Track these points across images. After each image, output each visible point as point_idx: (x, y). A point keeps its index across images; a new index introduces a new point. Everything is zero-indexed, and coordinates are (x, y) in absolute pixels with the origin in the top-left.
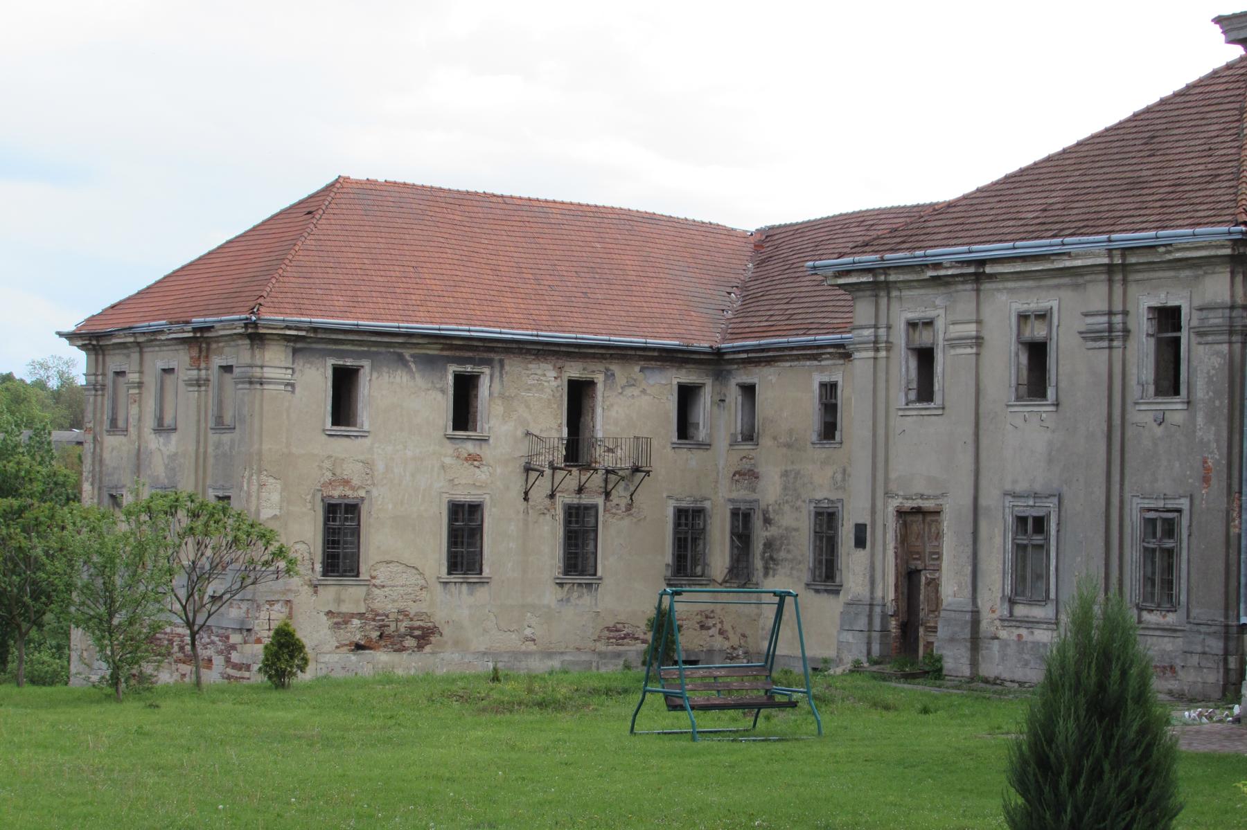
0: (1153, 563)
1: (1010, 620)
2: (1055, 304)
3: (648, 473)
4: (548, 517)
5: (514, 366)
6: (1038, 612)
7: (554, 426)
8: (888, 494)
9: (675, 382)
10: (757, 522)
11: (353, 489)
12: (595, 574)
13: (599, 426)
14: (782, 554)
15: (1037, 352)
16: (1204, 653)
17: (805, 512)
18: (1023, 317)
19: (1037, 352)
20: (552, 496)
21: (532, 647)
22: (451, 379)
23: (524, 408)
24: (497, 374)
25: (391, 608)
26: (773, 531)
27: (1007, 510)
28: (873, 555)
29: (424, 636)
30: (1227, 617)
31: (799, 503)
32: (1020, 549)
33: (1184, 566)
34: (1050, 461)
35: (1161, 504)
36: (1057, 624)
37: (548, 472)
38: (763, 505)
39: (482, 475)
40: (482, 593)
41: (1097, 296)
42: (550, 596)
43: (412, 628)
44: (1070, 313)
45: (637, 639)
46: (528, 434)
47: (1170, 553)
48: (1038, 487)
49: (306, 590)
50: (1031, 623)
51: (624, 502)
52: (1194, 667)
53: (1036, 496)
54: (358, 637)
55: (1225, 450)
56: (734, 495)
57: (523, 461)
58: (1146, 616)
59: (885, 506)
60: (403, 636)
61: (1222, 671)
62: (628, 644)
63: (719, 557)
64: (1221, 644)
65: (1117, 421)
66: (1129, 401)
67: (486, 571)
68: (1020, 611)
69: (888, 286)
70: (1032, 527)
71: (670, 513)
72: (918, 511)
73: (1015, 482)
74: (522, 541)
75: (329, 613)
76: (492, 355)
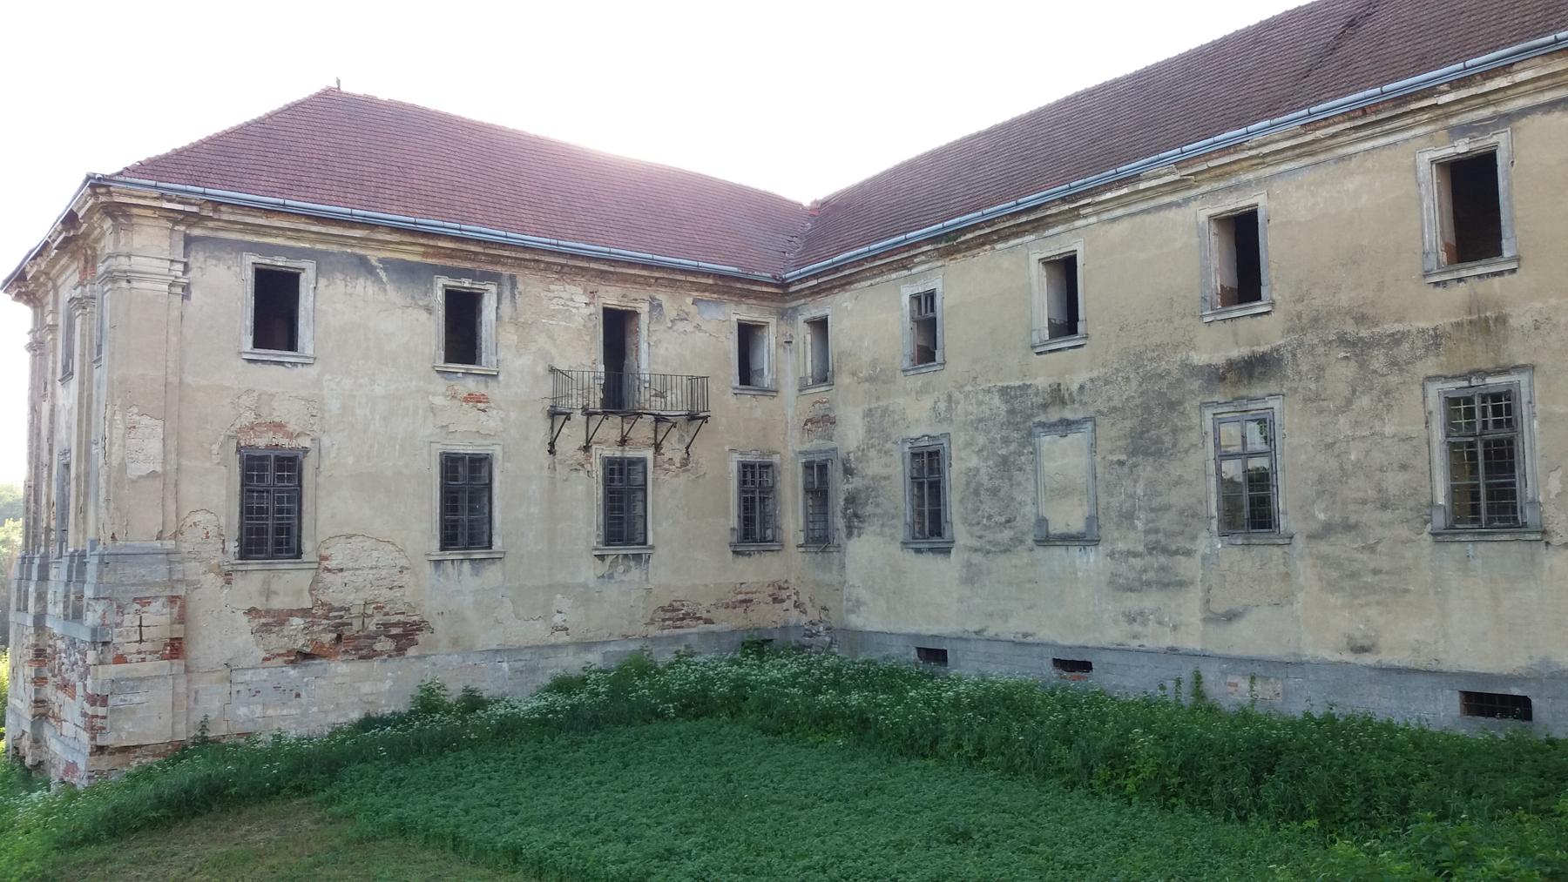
3: (705, 419)
4: (582, 474)
5: (530, 285)
7: (585, 357)
9: (734, 318)
10: (835, 473)
11: (290, 436)
12: (645, 543)
13: (644, 365)
14: (869, 509)
17: (897, 456)
20: (586, 448)
21: (562, 638)
22: (439, 297)
23: (544, 332)
24: (507, 293)
25: (354, 599)
26: (856, 483)
29: (406, 635)
31: (889, 445)
37: (578, 417)
38: (842, 453)
39: (491, 422)
42: (588, 571)
43: (387, 626)
45: (700, 618)
46: (552, 370)
49: (211, 581)
51: (678, 457)
54: (300, 643)
56: (807, 447)
57: (548, 404)
60: (373, 637)
62: (689, 626)
63: (791, 515)
67: (497, 543)
71: (733, 468)
74: (546, 502)
75: (252, 612)
76: (499, 269)
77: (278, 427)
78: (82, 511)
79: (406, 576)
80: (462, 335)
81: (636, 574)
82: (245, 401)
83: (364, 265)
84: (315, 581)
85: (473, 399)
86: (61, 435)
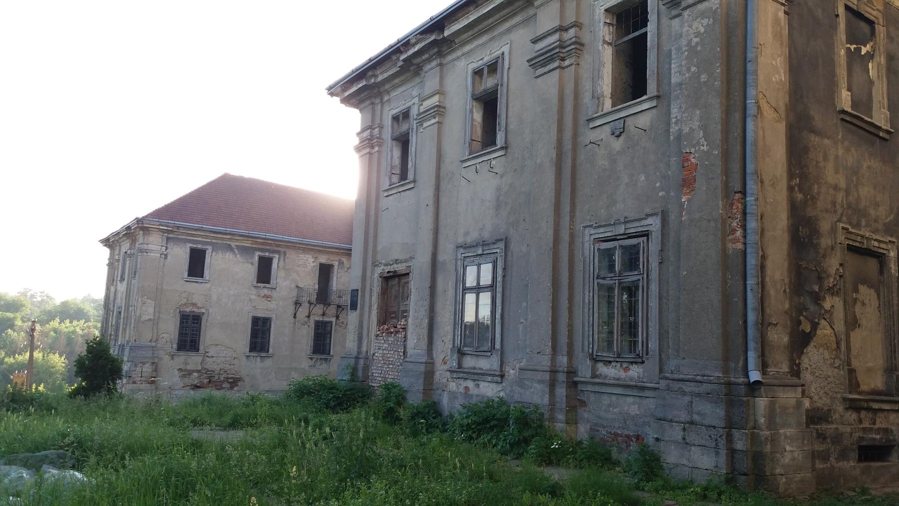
0: (610, 303)
1: (459, 372)
2: (506, 49)
5: (291, 255)
6: (484, 364)
7: (311, 283)
8: (375, 265)
11: (198, 308)
13: (334, 285)
15: (489, 104)
16: (692, 423)
19: (489, 104)
20: (309, 317)
22: (257, 258)
24: (282, 258)
25: (217, 368)
27: (459, 263)
28: (361, 316)
29: (234, 382)
30: (726, 371)
33: (654, 303)
34: (498, 207)
35: (621, 230)
36: (502, 376)
37: (307, 305)
39: (272, 305)
40: (268, 362)
46: (298, 287)
47: (631, 290)
48: (486, 235)
49: (167, 358)
50: (477, 375)
52: (676, 442)
53: (484, 244)
55: (718, 137)
57: (295, 299)
58: (602, 369)
59: (373, 273)
60: (223, 382)
61: (723, 452)
64: (721, 412)
65: (568, 146)
66: (582, 119)
67: (271, 350)
73: (467, 234)
74: (291, 338)
77: (194, 305)
78: (124, 330)
79: (236, 361)
80: (264, 274)
81: (324, 366)
82: (184, 295)
83: (229, 248)
84: (203, 360)
85: (266, 297)
86: (118, 301)
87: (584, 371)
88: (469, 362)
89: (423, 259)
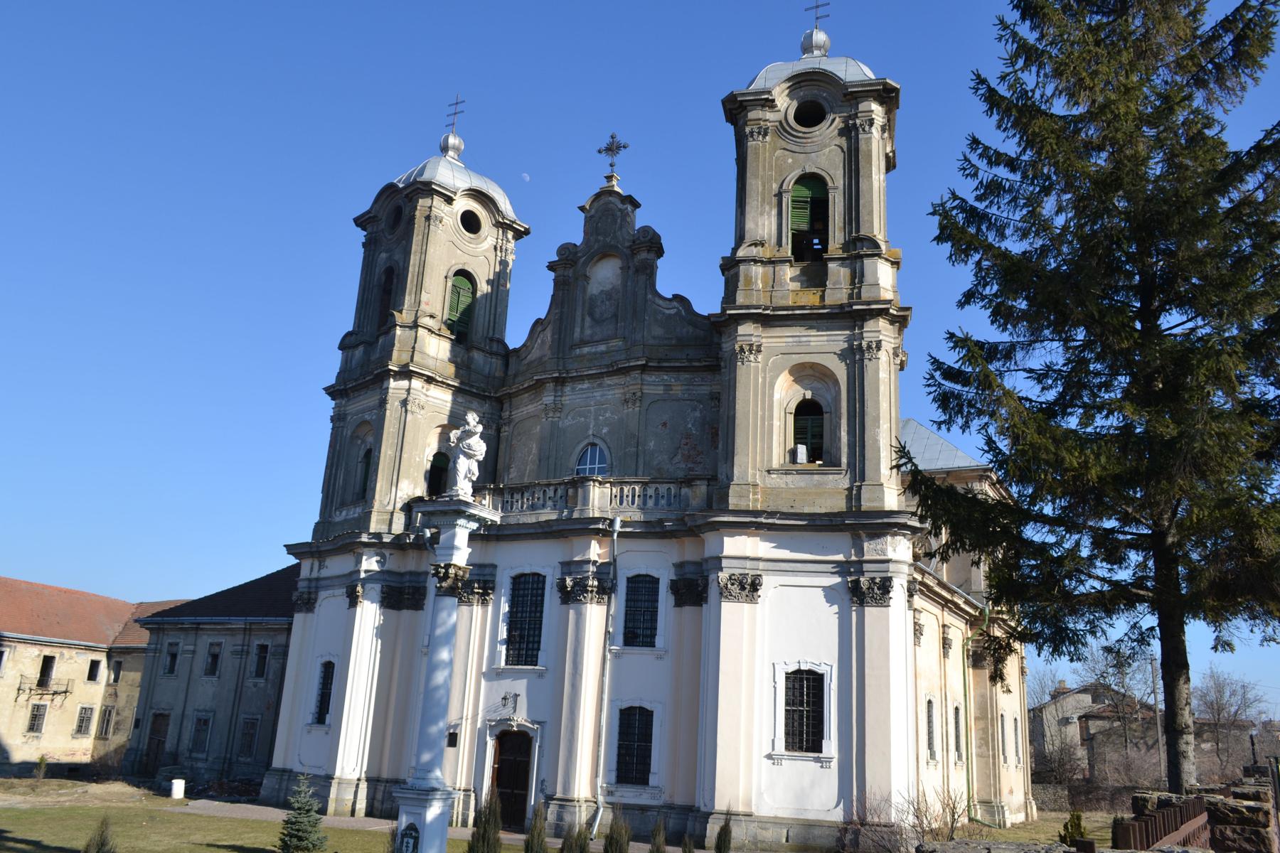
6: (203, 756)
7: (34, 672)
8: (151, 708)
15: (215, 657)
18: (211, 644)
19: (215, 657)
32: (197, 730)
41: (239, 639)
44: (229, 644)
68: (194, 755)
69: (163, 630)
70: (202, 723)
72: (161, 715)
87: (234, 759)
88: (194, 755)
89: (178, 711)
